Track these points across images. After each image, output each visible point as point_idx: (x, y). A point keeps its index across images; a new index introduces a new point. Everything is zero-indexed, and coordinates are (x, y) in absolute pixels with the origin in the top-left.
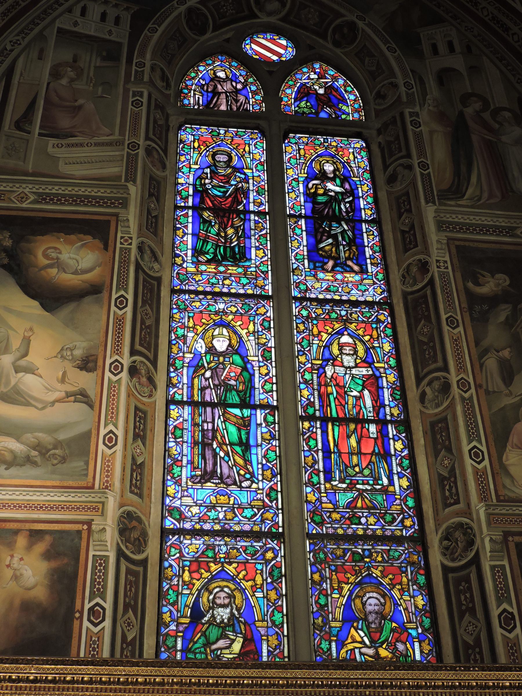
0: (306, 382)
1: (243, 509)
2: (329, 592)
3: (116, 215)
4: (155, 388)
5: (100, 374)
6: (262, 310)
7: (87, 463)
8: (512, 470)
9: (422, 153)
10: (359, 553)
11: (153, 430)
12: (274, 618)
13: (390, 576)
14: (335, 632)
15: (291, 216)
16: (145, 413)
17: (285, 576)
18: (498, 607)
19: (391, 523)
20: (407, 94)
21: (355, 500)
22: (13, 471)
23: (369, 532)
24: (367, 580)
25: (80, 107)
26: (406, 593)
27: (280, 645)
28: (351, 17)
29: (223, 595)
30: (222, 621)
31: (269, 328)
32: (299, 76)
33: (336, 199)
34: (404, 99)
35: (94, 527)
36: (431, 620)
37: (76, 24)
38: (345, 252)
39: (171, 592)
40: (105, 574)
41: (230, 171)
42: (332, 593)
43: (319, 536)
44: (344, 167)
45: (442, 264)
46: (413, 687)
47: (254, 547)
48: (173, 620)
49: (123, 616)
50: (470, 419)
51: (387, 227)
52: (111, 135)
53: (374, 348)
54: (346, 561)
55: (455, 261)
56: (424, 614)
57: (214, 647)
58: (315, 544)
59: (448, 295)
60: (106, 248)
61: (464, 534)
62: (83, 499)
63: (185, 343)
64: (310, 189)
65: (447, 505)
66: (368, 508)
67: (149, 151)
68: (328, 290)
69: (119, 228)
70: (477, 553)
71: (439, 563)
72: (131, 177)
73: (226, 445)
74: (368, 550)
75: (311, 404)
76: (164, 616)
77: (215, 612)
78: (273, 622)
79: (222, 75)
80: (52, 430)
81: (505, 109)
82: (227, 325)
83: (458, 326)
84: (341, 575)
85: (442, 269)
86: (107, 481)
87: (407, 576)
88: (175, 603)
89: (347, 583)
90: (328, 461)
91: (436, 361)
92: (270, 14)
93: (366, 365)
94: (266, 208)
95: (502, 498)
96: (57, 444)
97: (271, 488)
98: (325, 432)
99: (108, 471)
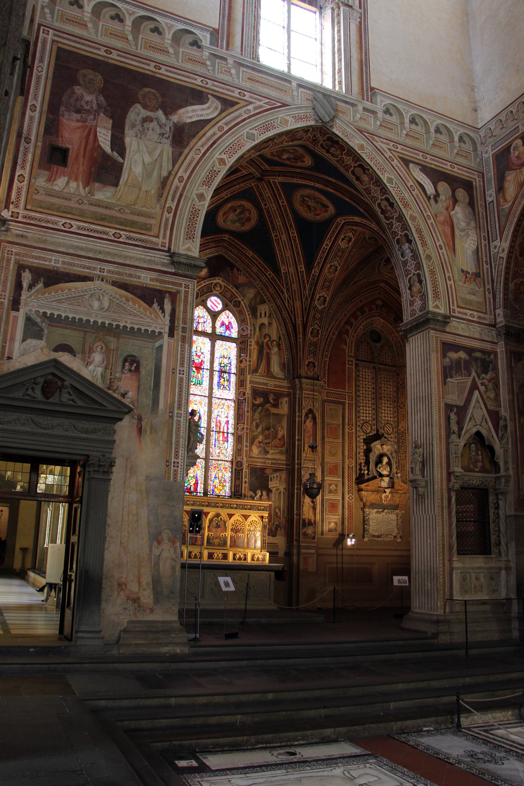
9: (250, 357)
28: (240, 299)
81: (274, 341)
92: (217, 291)
94: (209, 368)
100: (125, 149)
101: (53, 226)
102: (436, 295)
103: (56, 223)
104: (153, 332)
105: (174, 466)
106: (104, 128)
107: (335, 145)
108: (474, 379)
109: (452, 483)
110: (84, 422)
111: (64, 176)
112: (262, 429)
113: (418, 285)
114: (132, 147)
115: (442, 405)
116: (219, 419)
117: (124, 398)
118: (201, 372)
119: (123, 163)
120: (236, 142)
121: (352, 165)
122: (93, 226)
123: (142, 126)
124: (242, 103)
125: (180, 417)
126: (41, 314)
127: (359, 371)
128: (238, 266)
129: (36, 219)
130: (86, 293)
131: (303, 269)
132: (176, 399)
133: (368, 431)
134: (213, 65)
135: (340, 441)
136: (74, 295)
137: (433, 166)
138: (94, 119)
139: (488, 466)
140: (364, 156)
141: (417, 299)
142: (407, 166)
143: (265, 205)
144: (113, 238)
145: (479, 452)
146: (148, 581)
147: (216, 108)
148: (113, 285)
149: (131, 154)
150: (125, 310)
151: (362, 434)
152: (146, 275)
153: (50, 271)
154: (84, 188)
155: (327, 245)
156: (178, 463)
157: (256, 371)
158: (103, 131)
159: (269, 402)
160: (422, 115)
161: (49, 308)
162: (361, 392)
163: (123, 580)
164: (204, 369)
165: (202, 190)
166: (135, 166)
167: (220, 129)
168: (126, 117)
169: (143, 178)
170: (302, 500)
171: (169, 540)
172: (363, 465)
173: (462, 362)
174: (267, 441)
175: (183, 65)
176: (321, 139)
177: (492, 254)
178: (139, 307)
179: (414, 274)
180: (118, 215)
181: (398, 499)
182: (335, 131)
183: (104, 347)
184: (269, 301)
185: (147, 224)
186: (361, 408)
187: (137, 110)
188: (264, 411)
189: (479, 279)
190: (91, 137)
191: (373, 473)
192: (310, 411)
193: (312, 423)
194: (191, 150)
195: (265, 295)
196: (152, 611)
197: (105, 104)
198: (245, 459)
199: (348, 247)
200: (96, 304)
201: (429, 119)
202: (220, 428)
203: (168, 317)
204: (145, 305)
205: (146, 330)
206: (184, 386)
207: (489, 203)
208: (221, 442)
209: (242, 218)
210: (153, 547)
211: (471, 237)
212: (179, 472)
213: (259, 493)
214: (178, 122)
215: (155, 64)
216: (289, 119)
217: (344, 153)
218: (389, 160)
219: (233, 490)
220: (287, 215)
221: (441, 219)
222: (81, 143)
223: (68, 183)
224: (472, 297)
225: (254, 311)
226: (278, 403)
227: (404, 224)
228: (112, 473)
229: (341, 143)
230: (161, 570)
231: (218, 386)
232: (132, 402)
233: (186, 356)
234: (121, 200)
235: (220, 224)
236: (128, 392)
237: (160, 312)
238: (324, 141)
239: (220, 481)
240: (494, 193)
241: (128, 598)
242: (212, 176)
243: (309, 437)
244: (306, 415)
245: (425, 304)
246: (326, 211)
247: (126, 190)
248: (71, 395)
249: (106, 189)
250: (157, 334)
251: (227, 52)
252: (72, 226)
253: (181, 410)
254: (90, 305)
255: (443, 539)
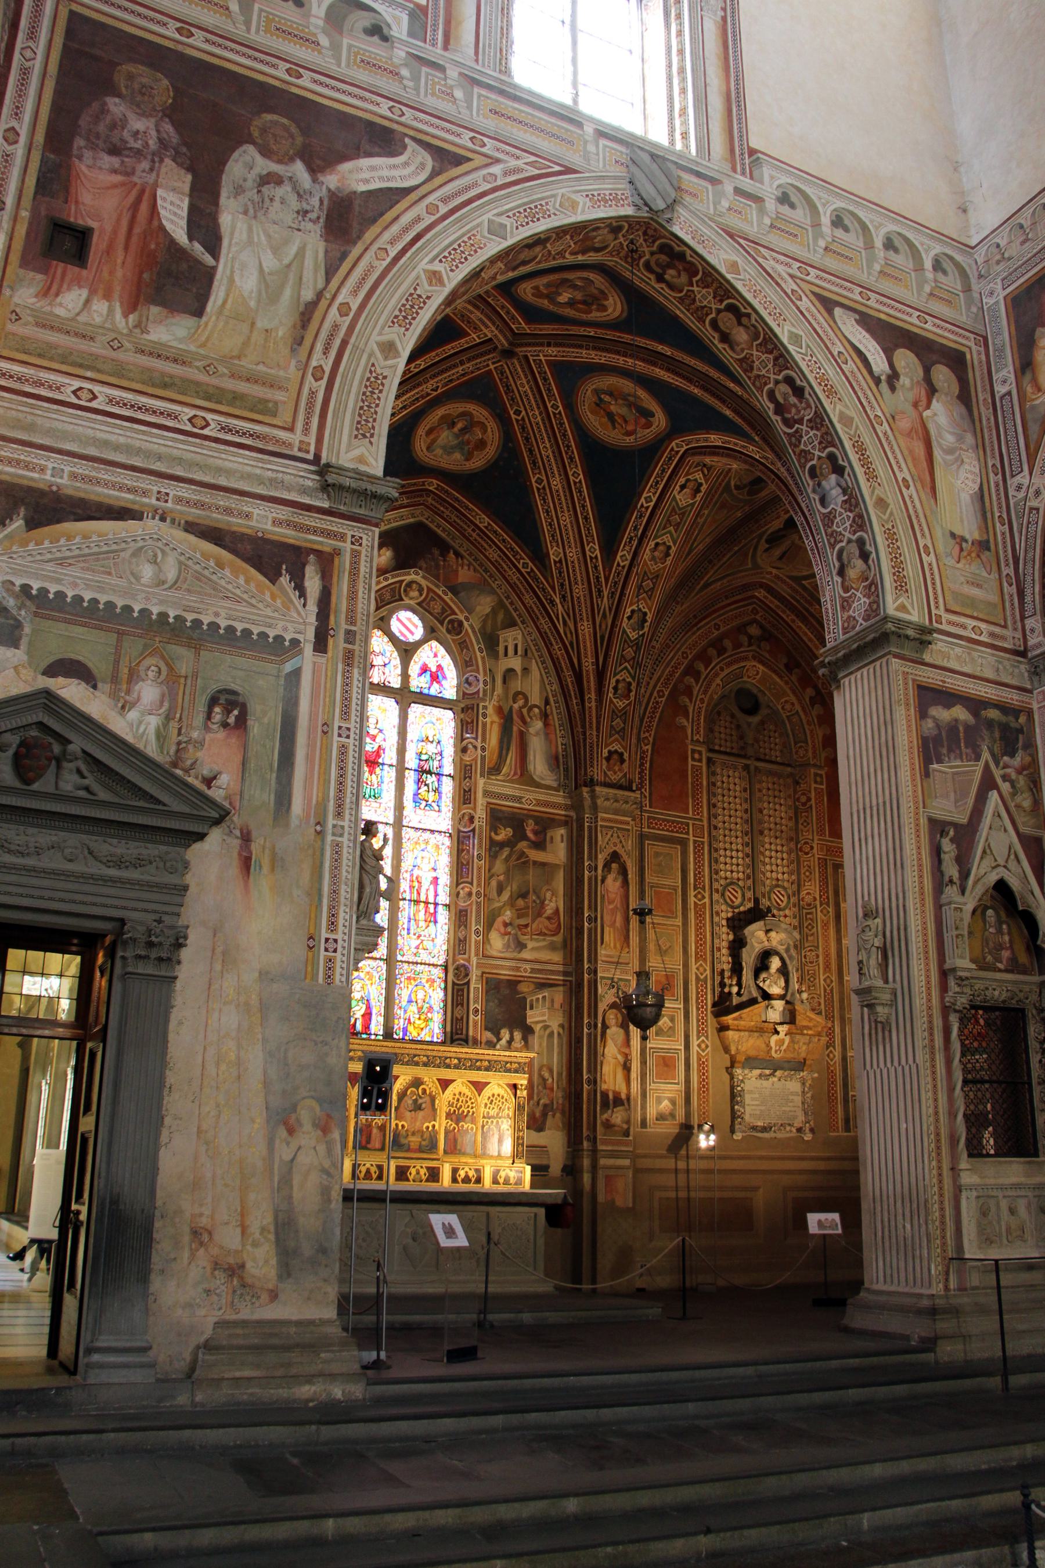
9: (484, 740)
28: (461, 617)
81: (536, 706)
100: (218, 239)
101: (50, 395)
102: (901, 585)
103: (58, 388)
104: (279, 638)
105: (326, 950)
106: (174, 190)
107: (677, 263)
108: (987, 766)
109: (950, 994)
110: (115, 841)
111: (80, 287)
112: (511, 896)
113: (859, 563)
114: (236, 235)
115: (923, 822)
116: (416, 872)
117: (209, 788)
118: (378, 770)
119: (214, 269)
120: (465, 239)
121: (713, 306)
122: (143, 400)
123: (259, 192)
124: (479, 161)
125: (341, 835)
126: (17, 589)
127: (714, 774)
128: (457, 547)
129: (11, 377)
130: (123, 545)
131: (598, 552)
132: (332, 793)
133: (737, 902)
134: (416, 78)
135: (679, 922)
136: (96, 550)
137: (883, 316)
138: (152, 169)
139: (1023, 958)
140: (739, 286)
141: (859, 594)
142: (830, 312)
143: (518, 413)
144: (188, 427)
145: (1004, 926)
146: (265, 1222)
147: (423, 166)
148: (186, 531)
149: (234, 249)
150: (215, 587)
151: (724, 907)
152: (262, 513)
153: (42, 493)
154: (126, 316)
155: (648, 500)
156: (336, 941)
157: (495, 770)
158: (171, 197)
159: (525, 837)
160: (856, 211)
161: (37, 576)
162: (720, 818)
163: (204, 1221)
165: (392, 334)
166: (242, 276)
167: (431, 209)
168: (222, 171)
169: (259, 302)
170: (600, 1050)
171: (315, 1125)
172: (727, 974)
173: (961, 729)
174: (523, 921)
175: (351, 73)
176: (646, 250)
177: (1012, 502)
178: (247, 582)
179: (849, 541)
180: (203, 378)
181: (804, 1048)
182: (676, 229)
183: (164, 669)
184: (523, 622)
185: (267, 401)
186: (722, 852)
187: (248, 158)
188: (514, 857)
189: (987, 553)
190: (144, 207)
191: (750, 992)
192: (615, 857)
193: (618, 883)
194: (366, 249)
195: (516, 610)
196: (274, 1295)
197: (175, 139)
198: (474, 960)
199: (693, 505)
200: (147, 572)
201: (872, 221)
202: (419, 894)
203: (312, 608)
204: (261, 577)
205: (263, 635)
206: (350, 765)
207: (1002, 398)
208: (422, 924)
209: (468, 442)
210: (277, 1142)
211: (966, 467)
212: (338, 964)
213: (505, 1035)
214: (338, 188)
215: (288, 66)
216: (580, 199)
217: (694, 280)
218: (792, 297)
219: (448, 1029)
220: (564, 435)
221: (904, 424)
222: (119, 220)
223: (87, 301)
224: (975, 592)
225: (491, 643)
226: (545, 840)
227: (827, 433)
228: (179, 962)
229: (689, 258)
230: (296, 1194)
232: (228, 797)
233: (354, 695)
234: (209, 345)
235: (420, 453)
236: (220, 773)
237: (294, 595)
238: (652, 254)
239: (420, 1009)
240: (1012, 376)
241: (216, 1265)
242: (412, 307)
243: (613, 912)
244: (605, 866)
245: (877, 603)
246: (649, 425)
247: (221, 324)
248: (84, 777)
249: (174, 321)
250: (287, 643)
251: (446, 54)
252: (95, 397)
253: (343, 820)
254: (132, 574)
255: (937, 1120)
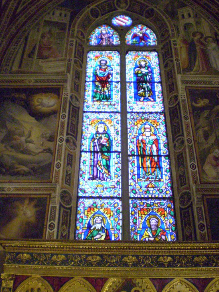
0: (132, 142)
1: (107, 189)
2: (137, 218)
3: (63, 85)
4: (76, 146)
5: (55, 142)
6: (116, 117)
7: (50, 174)
8: (206, 172)
9: (177, 55)
10: (149, 204)
11: (75, 162)
12: (117, 227)
13: (161, 212)
14: (139, 232)
15: (128, 82)
16: (72, 155)
17: (121, 212)
18: (198, 222)
19: (161, 193)
20: (172, 33)
21: (149, 184)
22: (24, 178)
23: (153, 196)
24: (152, 213)
25: (50, 48)
26: (166, 218)
27: (118, 237)
28: (152, 7)
29: (99, 219)
30: (98, 229)
31: (119, 123)
32: (133, 30)
33: (145, 75)
34: (171, 35)
35: (51, 196)
36: (175, 227)
37: (51, 18)
38: (148, 94)
39: (80, 219)
40: (55, 213)
41: (106, 67)
42: (138, 218)
43: (134, 198)
44: (149, 63)
45: (183, 96)
46: (154, 249)
47: (110, 202)
48: (81, 228)
49: (61, 227)
50: (191, 153)
51: (164, 84)
52: (62, 56)
53: (157, 129)
54: (144, 207)
55: (188, 94)
56: (173, 225)
57: (95, 238)
58: (133, 201)
59: (185, 107)
60: (59, 98)
61: (188, 196)
62: (48, 186)
63: (88, 130)
64: (135, 72)
65: (182, 185)
66: (153, 187)
67: (75, 62)
68: (141, 108)
69: (64, 90)
70: (192, 202)
71: (179, 207)
72: (68, 71)
73: (102, 166)
74: (153, 203)
75: (133, 150)
76: (78, 227)
77: (96, 226)
78: (117, 229)
79: (104, 32)
80: (38, 163)
81: (210, 37)
82: (103, 123)
83: (188, 119)
84: (142, 212)
85: (183, 98)
86: (57, 180)
87: (167, 212)
88: (82, 222)
89: (144, 215)
90: (139, 171)
91: (179, 133)
92: (122, 8)
93: (154, 135)
94: (119, 79)
95: (202, 182)
96: (40, 168)
97: (118, 181)
98: (138, 160)
99: (57, 176)
116: (140, 138)
157: (189, 69)
164: (112, 82)
184: (191, 4)
198: (194, 187)
202: (144, 150)
231: (135, 97)
